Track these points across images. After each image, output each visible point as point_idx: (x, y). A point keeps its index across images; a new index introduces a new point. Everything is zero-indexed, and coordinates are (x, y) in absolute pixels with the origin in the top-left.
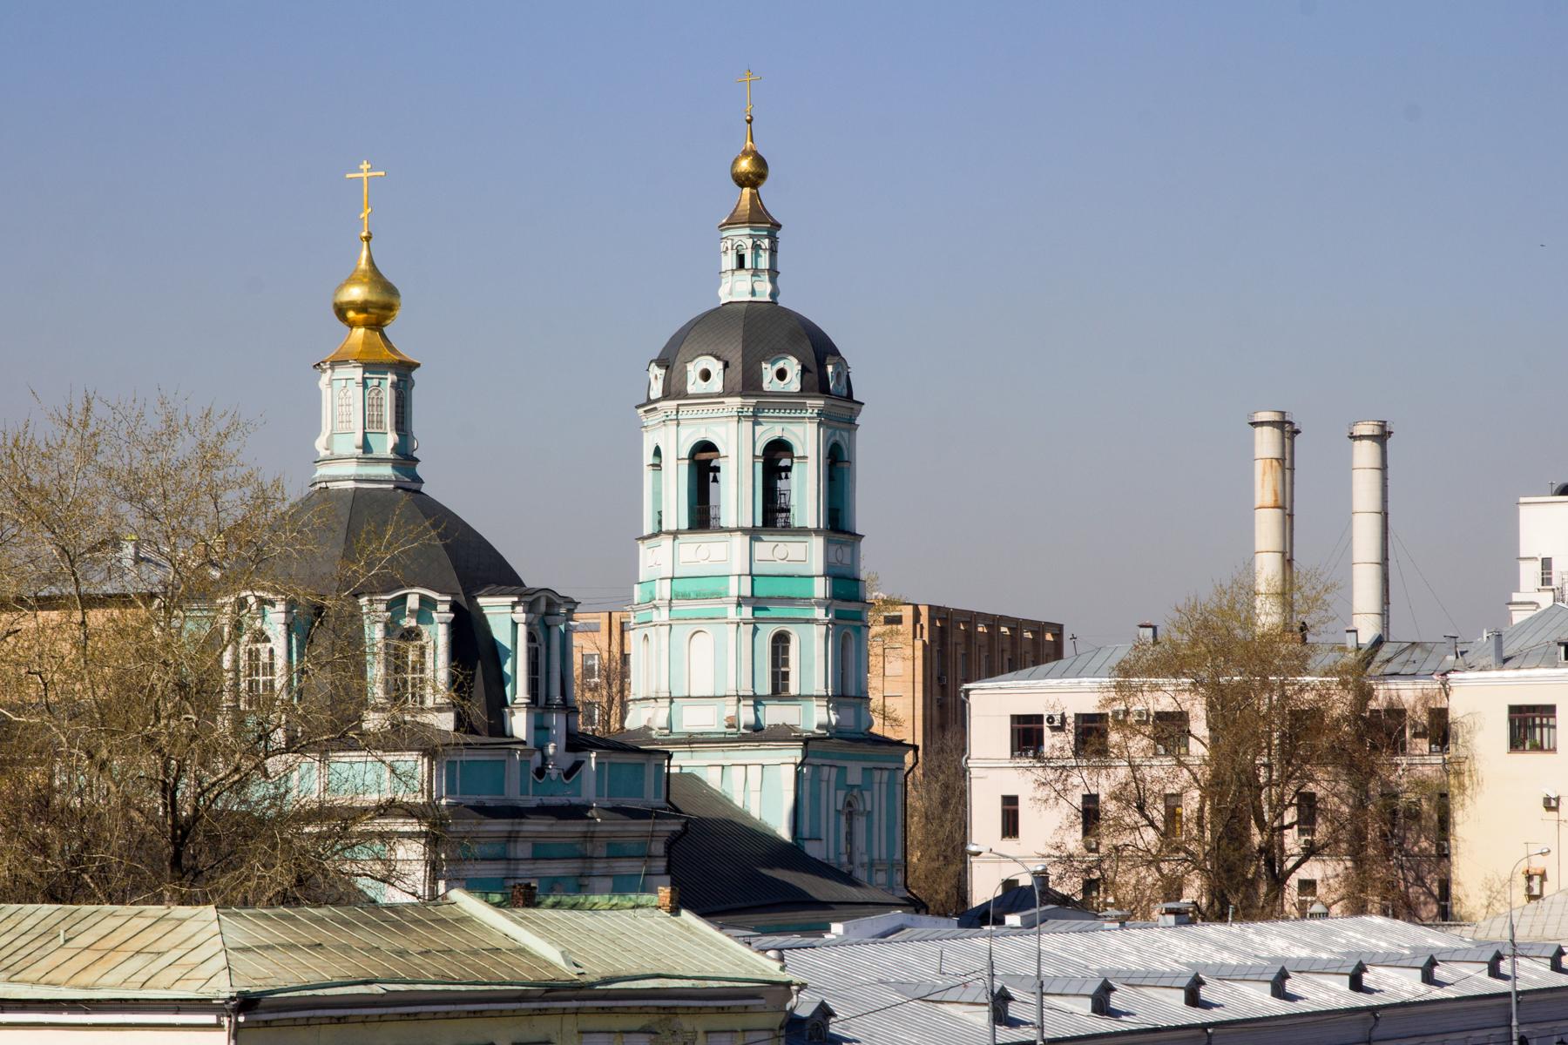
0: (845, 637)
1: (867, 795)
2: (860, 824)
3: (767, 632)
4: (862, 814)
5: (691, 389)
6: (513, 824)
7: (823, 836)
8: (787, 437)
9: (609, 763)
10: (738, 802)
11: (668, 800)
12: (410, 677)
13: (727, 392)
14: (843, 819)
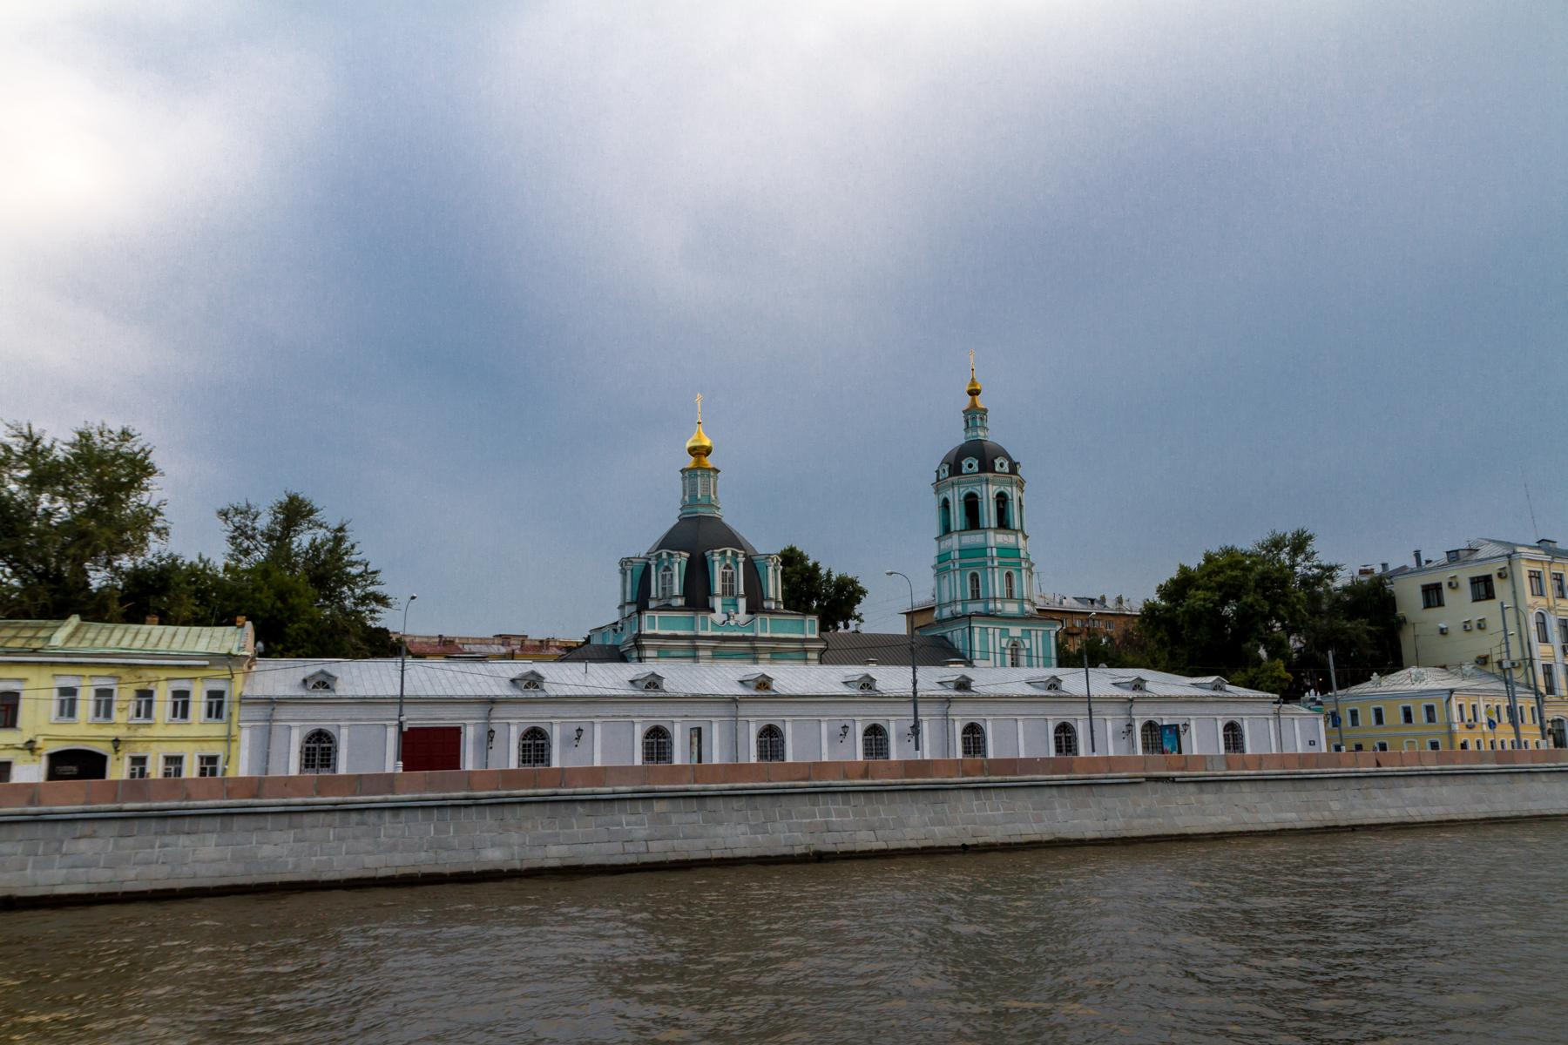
0: (1009, 575)
1: (1027, 642)
13: (950, 476)
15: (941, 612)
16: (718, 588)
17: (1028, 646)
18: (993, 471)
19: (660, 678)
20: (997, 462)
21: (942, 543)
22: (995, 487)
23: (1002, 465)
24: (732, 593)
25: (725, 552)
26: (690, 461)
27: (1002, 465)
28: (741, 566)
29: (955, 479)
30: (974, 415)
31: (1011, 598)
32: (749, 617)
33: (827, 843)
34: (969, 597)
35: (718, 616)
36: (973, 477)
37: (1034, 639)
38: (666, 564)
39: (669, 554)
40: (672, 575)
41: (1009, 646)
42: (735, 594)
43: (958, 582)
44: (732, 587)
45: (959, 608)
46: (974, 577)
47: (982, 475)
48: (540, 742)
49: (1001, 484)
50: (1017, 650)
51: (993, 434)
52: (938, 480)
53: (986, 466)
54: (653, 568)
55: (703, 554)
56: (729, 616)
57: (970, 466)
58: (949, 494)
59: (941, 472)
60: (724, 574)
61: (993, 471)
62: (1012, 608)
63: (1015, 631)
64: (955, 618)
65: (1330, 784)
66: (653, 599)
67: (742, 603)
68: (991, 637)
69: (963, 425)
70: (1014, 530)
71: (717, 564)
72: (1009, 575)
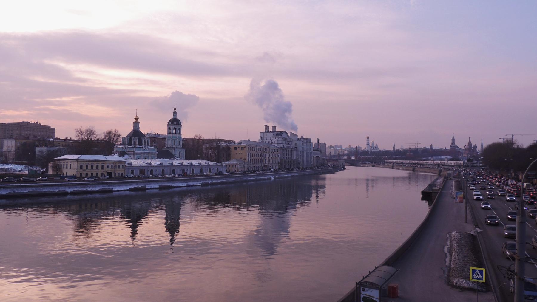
0: (180, 141)
2: (181, 154)
13: (171, 124)
28: (137, 140)
30: (175, 113)
51: (178, 117)
58: (171, 127)
64: (171, 148)
69: (173, 115)
72: (180, 141)
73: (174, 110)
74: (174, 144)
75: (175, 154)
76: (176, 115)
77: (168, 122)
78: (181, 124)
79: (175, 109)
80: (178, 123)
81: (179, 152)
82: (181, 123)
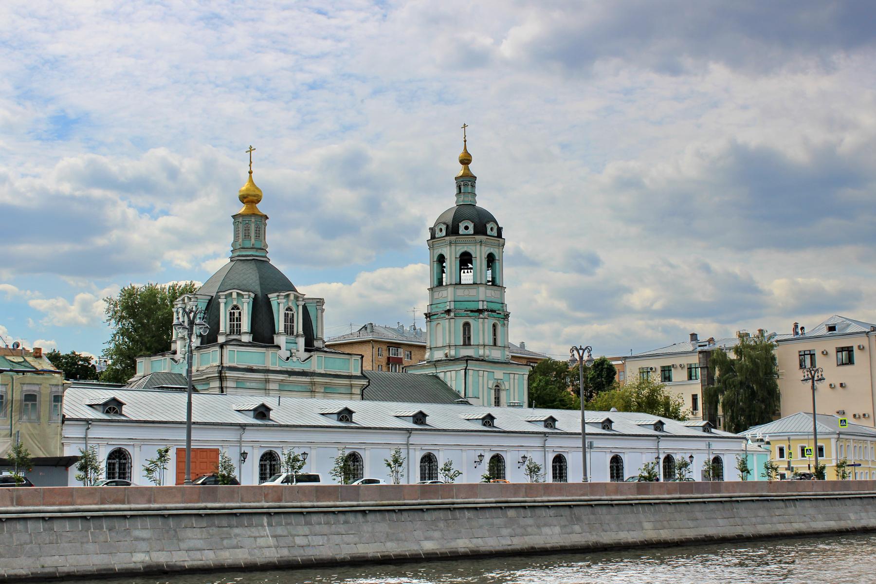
0: (494, 326)
1: (507, 384)
3: (461, 322)
4: (504, 390)
5: (437, 236)
6: (265, 376)
7: (481, 397)
8: (469, 250)
9: (325, 357)
10: (449, 385)
11: (362, 373)
12: (235, 323)
13: (447, 235)
14: (493, 392)
15: (432, 355)
16: (280, 326)
17: (507, 387)
18: (485, 234)
19: (268, 410)
20: (489, 226)
21: (436, 295)
22: (487, 248)
23: (492, 229)
24: (292, 333)
25: (288, 296)
26: (242, 209)
27: (492, 229)
28: (301, 308)
29: (453, 238)
30: (466, 183)
31: (495, 344)
32: (307, 355)
33: (299, 555)
34: (462, 344)
35: (284, 353)
36: (470, 238)
37: (512, 381)
38: (235, 303)
39: (238, 294)
40: (240, 313)
41: (494, 387)
42: (295, 333)
43: (452, 330)
44: (292, 327)
45: (453, 353)
46: (467, 325)
47: (476, 237)
48: (124, 461)
49: (492, 245)
50: (499, 390)
51: (481, 203)
52: (433, 237)
53: (480, 230)
54: (222, 306)
55: (267, 295)
56: (291, 353)
57: (466, 228)
58: (446, 251)
59: (437, 231)
60: (286, 315)
61: (485, 234)
62: (496, 354)
63: (499, 374)
64: (451, 360)
65: (848, 502)
66: (223, 334)
67: (301, 341)
68: (481, 378)
69: (455, 191)
70: (499, 286)
71: (281, 305)
73: (461, 166)
74: (467, 342)
75: (470, 393)
76: (473, 186)
77: (431, 229)
78: (499, 235)
79: (466, 161)
80: (480, 230)
81: (491, 384)
82: (500, 230)
